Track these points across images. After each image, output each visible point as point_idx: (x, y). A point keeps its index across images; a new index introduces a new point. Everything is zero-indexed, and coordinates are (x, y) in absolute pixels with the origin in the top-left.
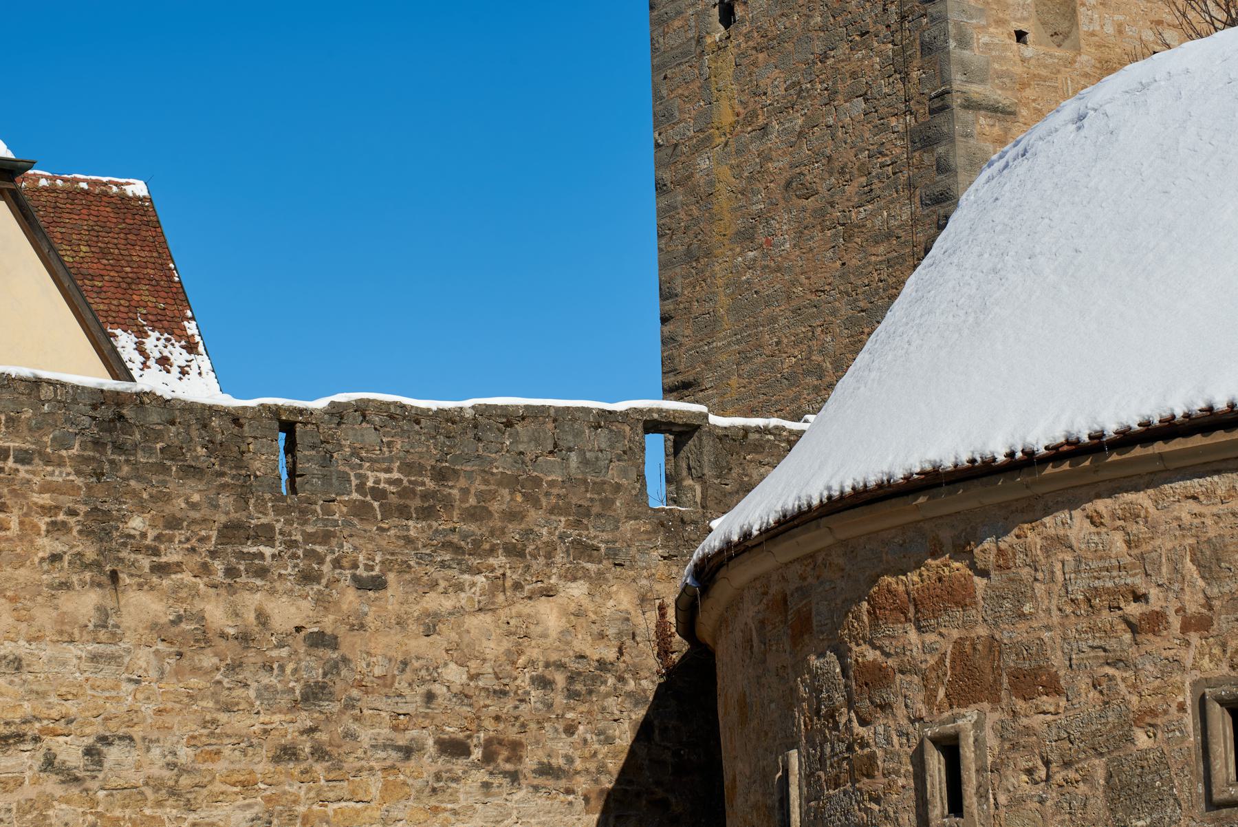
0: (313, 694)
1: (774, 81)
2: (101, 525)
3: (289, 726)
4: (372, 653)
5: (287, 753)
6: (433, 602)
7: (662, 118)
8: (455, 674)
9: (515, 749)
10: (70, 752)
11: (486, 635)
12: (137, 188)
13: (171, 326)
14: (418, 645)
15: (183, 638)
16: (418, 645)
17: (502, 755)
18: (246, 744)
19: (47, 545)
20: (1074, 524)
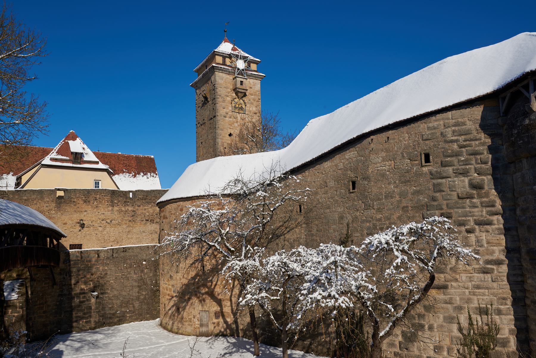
0: (133, 216)
1: (205, 151)
2: (112, 202)
3: (130, 219)
4: (139, 212)
5: (130, 221)
6: (145, 207)
7: (197, 154)
8: (147, 214)
9: (153, 220)
10: (109, 221)
11: (151, 211)
12: (152, 157)
13: (154, 172)
14: (144, 211)
15: (120, 211)
16: (144, 211)
17: (152, 221)
18: (126, 220)
19: (107, 203)
20: (168, 206)
